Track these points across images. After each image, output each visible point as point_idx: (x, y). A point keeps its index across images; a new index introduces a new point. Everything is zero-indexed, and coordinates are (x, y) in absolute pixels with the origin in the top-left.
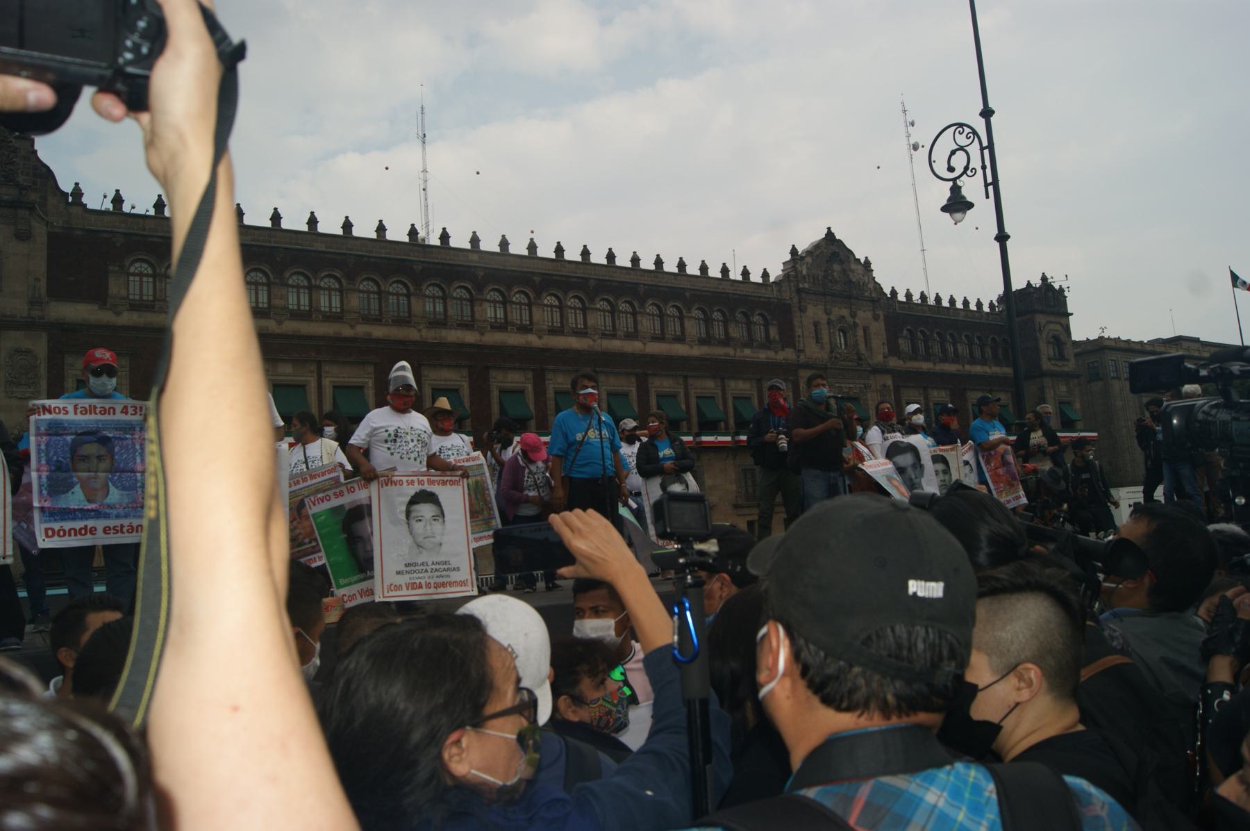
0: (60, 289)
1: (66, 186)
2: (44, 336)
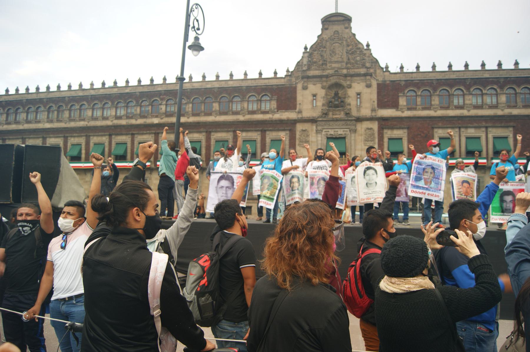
0: (382, 104)
1: (383, 65)
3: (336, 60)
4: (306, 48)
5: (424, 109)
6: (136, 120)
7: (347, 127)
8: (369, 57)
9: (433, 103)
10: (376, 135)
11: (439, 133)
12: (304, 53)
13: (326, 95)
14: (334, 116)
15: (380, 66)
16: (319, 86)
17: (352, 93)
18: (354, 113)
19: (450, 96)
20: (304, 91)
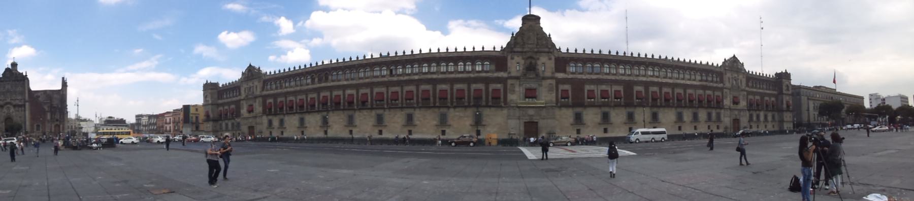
11: (587, 87)
17: (539, 62)
18: (541, 75)
19: (593, 67)
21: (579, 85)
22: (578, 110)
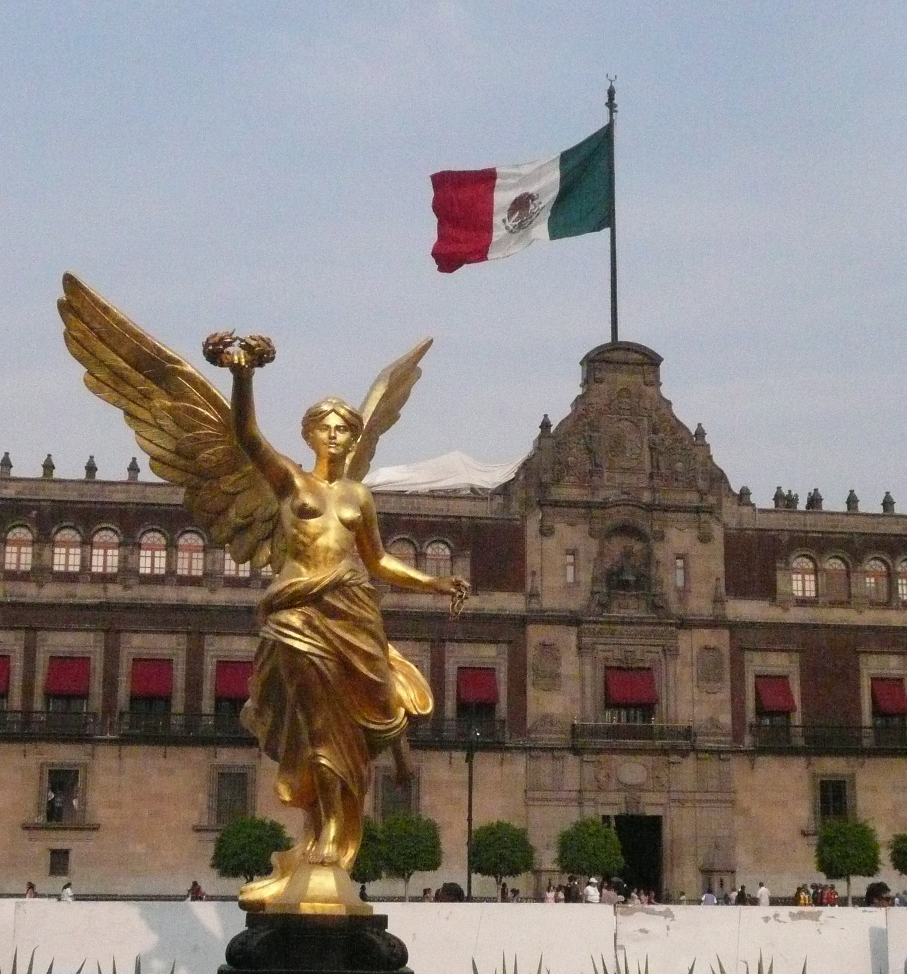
2: (726, 633)
3: (625, 465)
4: (545, 425)
5: (833, 604)
6: (41, 585)
7: (658, 642)
8: (704, 464)
9: (853, 590)
10: (727, 665)
12: (540, 437)
13: (601, 554)
14: (623, 613)
15: (730, 490)
16: (583, 528)
20: (545, 539)
21: (830, 654)
22: (833, 766)
